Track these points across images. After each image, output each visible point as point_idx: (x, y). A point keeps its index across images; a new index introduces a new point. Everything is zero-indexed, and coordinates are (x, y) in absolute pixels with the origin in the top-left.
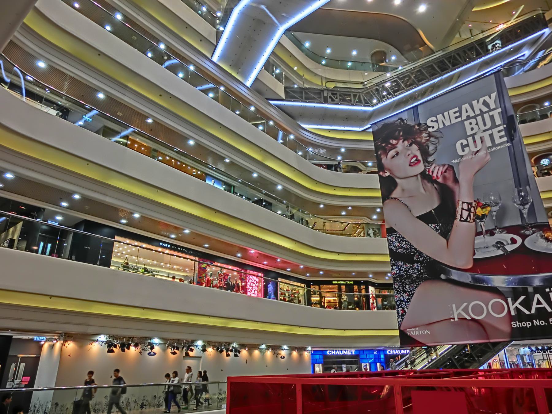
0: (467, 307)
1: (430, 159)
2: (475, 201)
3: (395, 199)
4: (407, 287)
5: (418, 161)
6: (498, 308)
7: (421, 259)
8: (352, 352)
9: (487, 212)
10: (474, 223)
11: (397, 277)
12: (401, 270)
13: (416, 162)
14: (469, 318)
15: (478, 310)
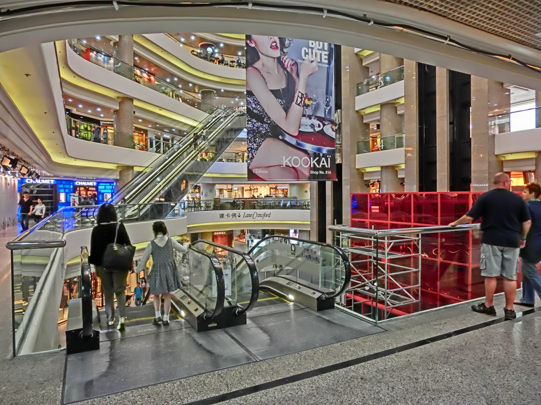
0: (291, 159)
1: (285, 50)
2: (306, 94)
3: (257, 69)
4: (257, 139)
5: (277, 48)
6: (306, 163)
7: (269, 122)
8: (50, 182)
9: (310, 104)
10: (302, 108)
11: (251, 130)
12: (254, 126)
13: (275, 47)
14: (291, 166)
15: (296, 162)
